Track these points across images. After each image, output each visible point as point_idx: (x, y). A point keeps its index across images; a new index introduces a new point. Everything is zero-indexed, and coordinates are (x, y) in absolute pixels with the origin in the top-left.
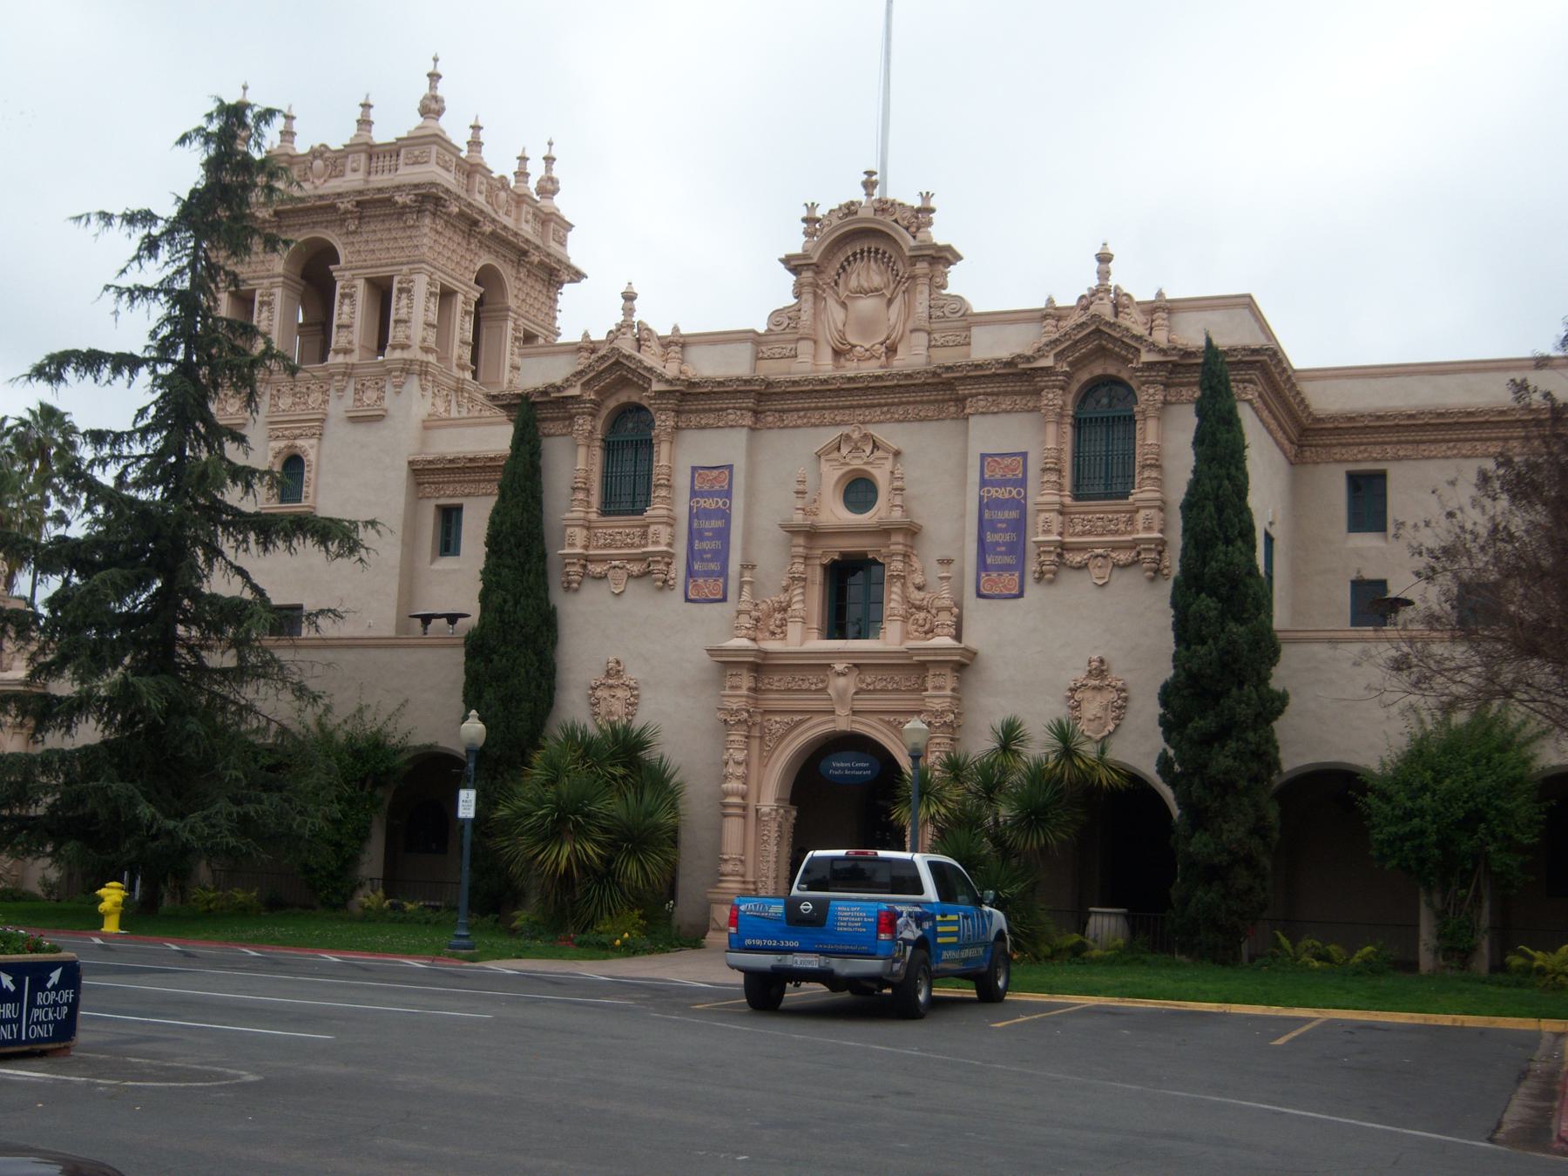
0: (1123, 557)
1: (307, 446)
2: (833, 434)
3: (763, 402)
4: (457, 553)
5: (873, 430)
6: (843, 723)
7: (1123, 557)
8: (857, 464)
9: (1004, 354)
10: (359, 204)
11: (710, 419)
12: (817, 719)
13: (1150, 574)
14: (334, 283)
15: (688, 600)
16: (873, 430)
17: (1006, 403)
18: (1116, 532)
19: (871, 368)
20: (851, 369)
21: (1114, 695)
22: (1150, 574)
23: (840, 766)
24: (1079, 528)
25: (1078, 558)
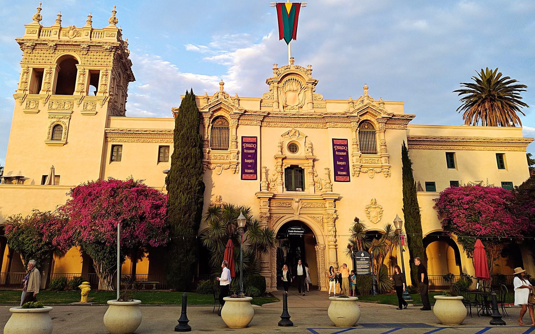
0: (378, 170)
2: (287, 130)
3: (265, 118)
4: (120, 160)
5: (301, 130)
6: (296, 218)
7: (378, 170)
8: (294, 139)
9: (342, 111)
11: (249, 122)
12: (288, 216)
13: (386, 175)
15: (242, 179)
16: (301, 130)
17: (339, 125)
18: (375, 163)
19: (294, 112)
20: (287, 111)
22: (386, 175)
23: (294, 231)
24: (364, 162)
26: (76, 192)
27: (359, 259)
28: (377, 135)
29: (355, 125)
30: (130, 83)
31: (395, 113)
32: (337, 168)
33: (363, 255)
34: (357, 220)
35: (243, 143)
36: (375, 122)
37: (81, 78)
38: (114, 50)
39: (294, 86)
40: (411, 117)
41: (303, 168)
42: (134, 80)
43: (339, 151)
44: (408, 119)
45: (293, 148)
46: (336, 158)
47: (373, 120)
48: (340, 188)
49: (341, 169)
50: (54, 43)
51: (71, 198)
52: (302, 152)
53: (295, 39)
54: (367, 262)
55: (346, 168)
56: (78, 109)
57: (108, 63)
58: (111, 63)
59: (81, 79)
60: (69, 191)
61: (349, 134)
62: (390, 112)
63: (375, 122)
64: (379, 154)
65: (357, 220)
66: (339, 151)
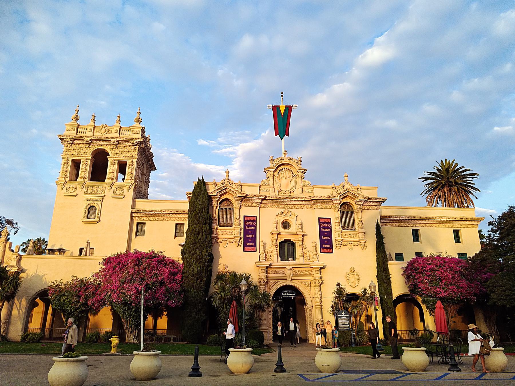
0: (356, 243)
1: (97, 204)
2: (281, 210)
6: (289, 283)
7: (356, 243)
8: (287, 218)
9: (327, 195)
10: (118, 141)
11: (250, 204)
14: (107, 161)
15: (244, 251)
17: (324, 206)
19: (287, 195)
20: (281, 195)
21: (357, 276)
23: (287, 294)
25: (345, 243)
26: (108, 261)
27: (340, 317)
28: (355, 214)
29: (337, 206)
30: (152, 171)
31: (370, 197)
32: (322, 242)
33: (343, 313)
34: (338, 285)
35: (245, 221)
36: (354, 204)
37: (112, 168)
38: (138, 144)
39: (287, 174)
40: (383, 199)
41: (294, 242)
42: (155, 169)
43: (324, 227)
44: (380, 202)
45: (286, 225)
46: (321, 233)
47: (352, 202)
48: (324, 258)
49: (326, 242)
50: (89, 139)
51: (103, 267)
52: (293, 229)
53: (288, 135)
54: (347, 319)
55: (330, 242)
56: (109, 193)
57: (134, 156)
58: (137, 156)
59: (112, 169)
60: (101, 261)
61: (332, 214)
62: (366, 195)
63: (354, 204)
64: (357, 230)
65: (338, 285)
66: (324, 227)
